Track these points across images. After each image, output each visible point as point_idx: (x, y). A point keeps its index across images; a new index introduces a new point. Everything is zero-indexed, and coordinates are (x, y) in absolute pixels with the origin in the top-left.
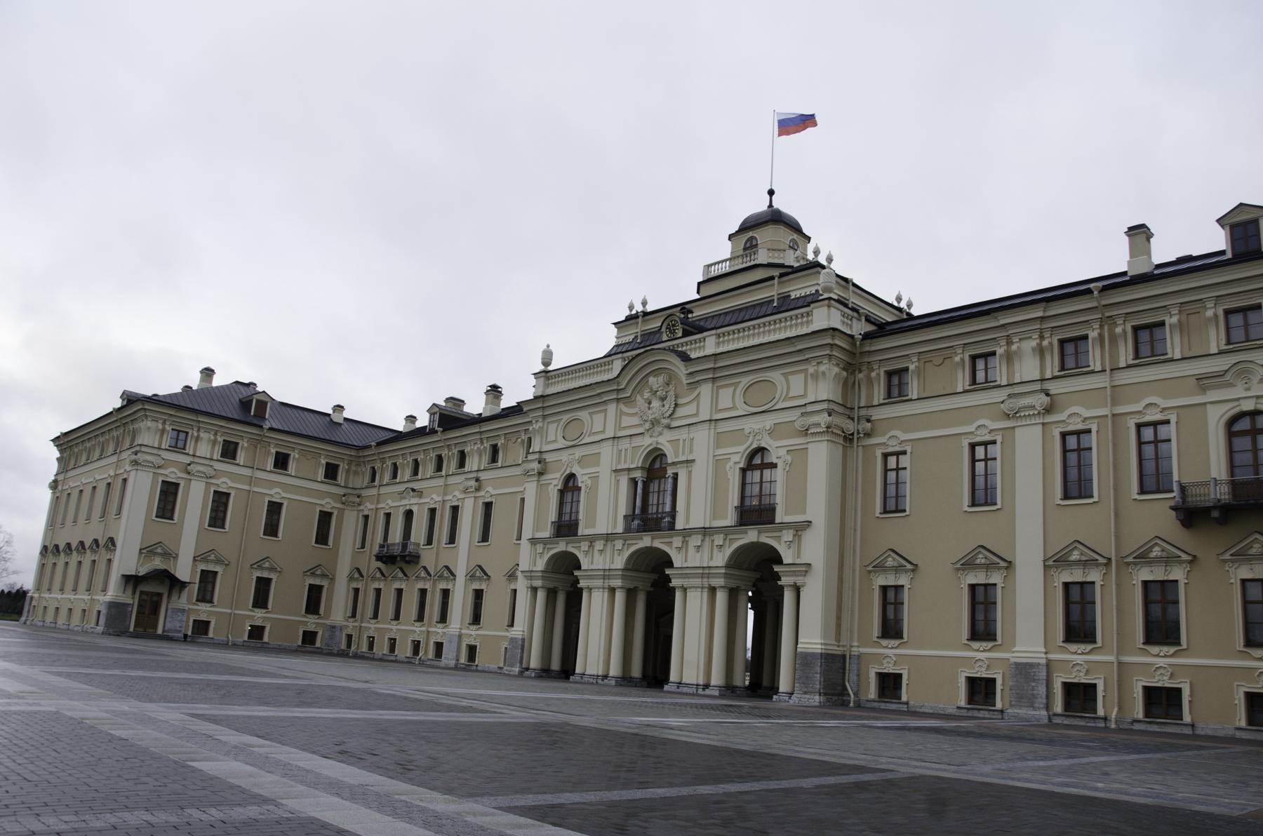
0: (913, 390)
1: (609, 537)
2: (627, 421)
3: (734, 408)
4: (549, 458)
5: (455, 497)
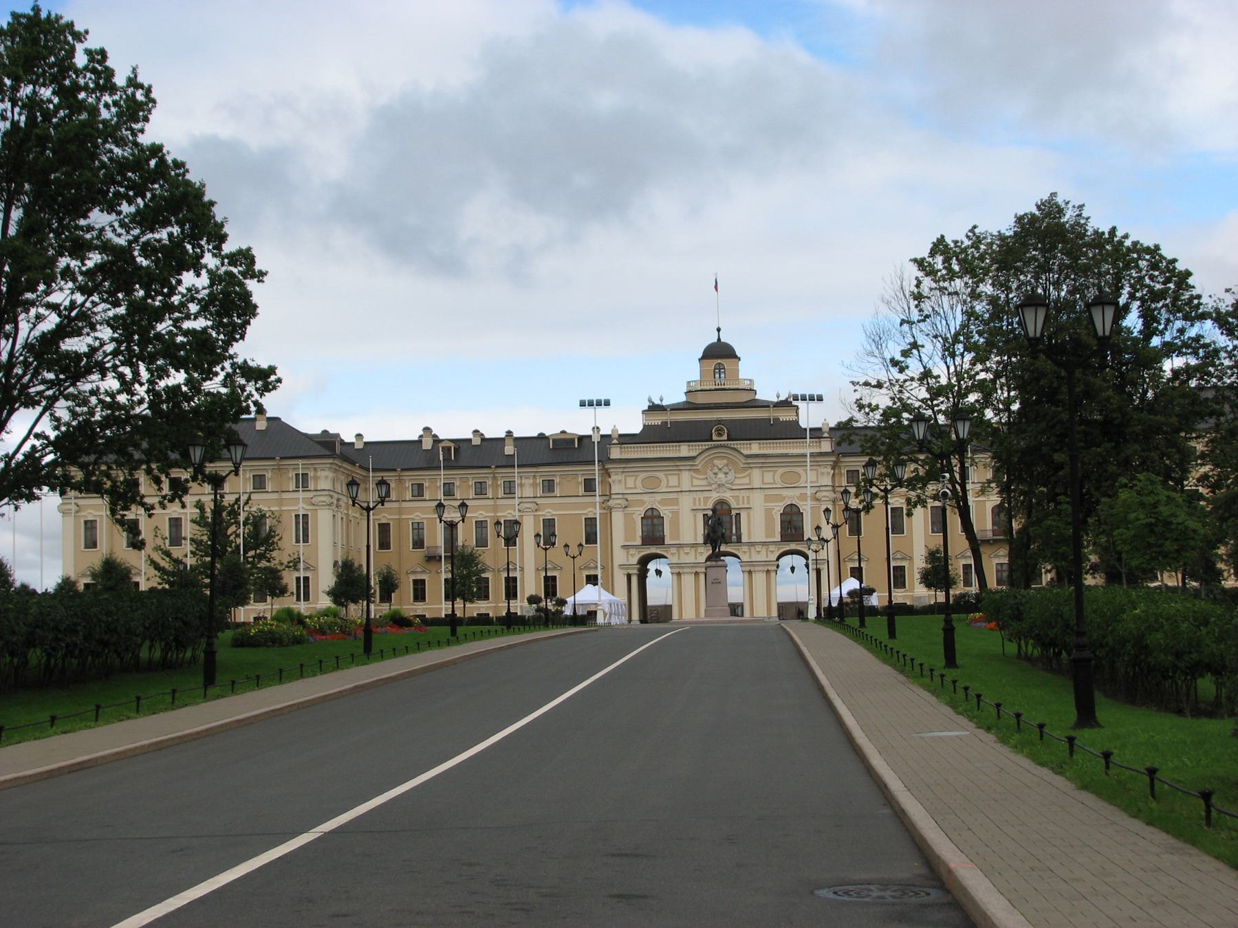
1: (694, 545)
2: (696, 482)
3: (774, 483)
4: (630, 498)
5: (508, 514)
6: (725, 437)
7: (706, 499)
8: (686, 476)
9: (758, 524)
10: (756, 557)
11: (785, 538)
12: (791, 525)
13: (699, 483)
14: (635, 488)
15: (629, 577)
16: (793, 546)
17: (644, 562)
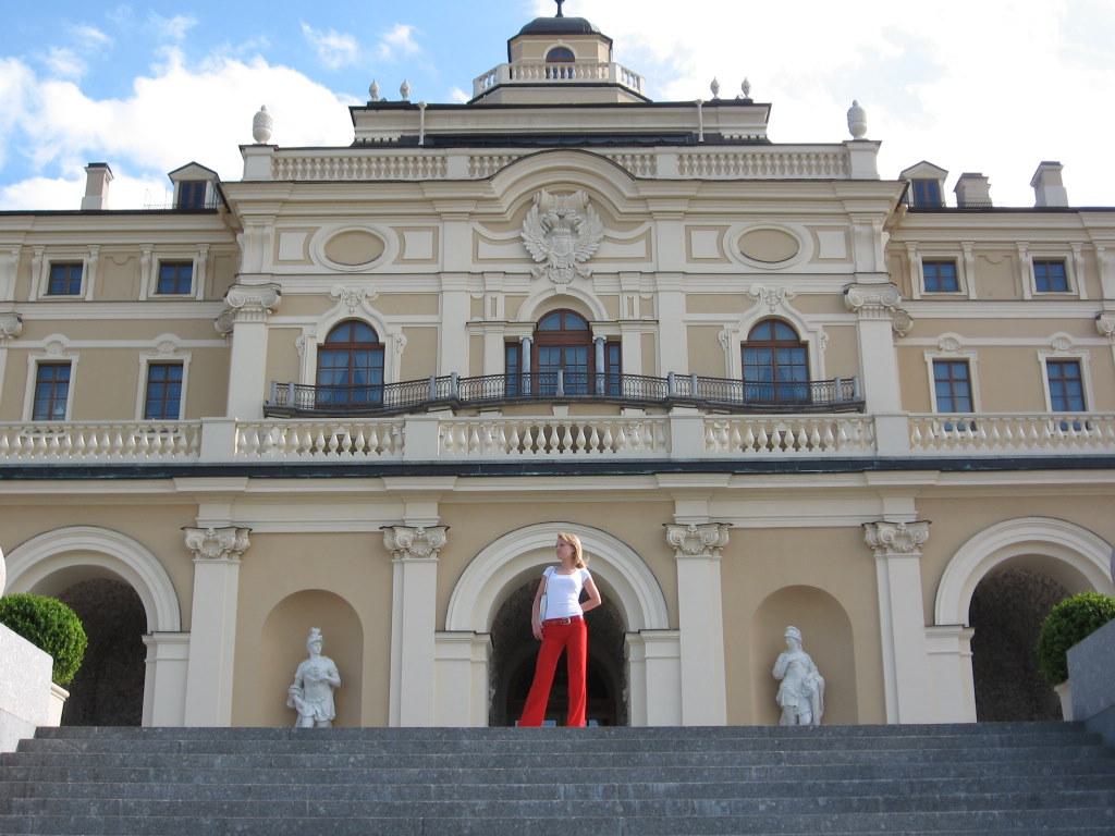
2: (486, 250)
4: (289, 287)
7: (516, 299)
13: (499, 249)
14: (308, 260)
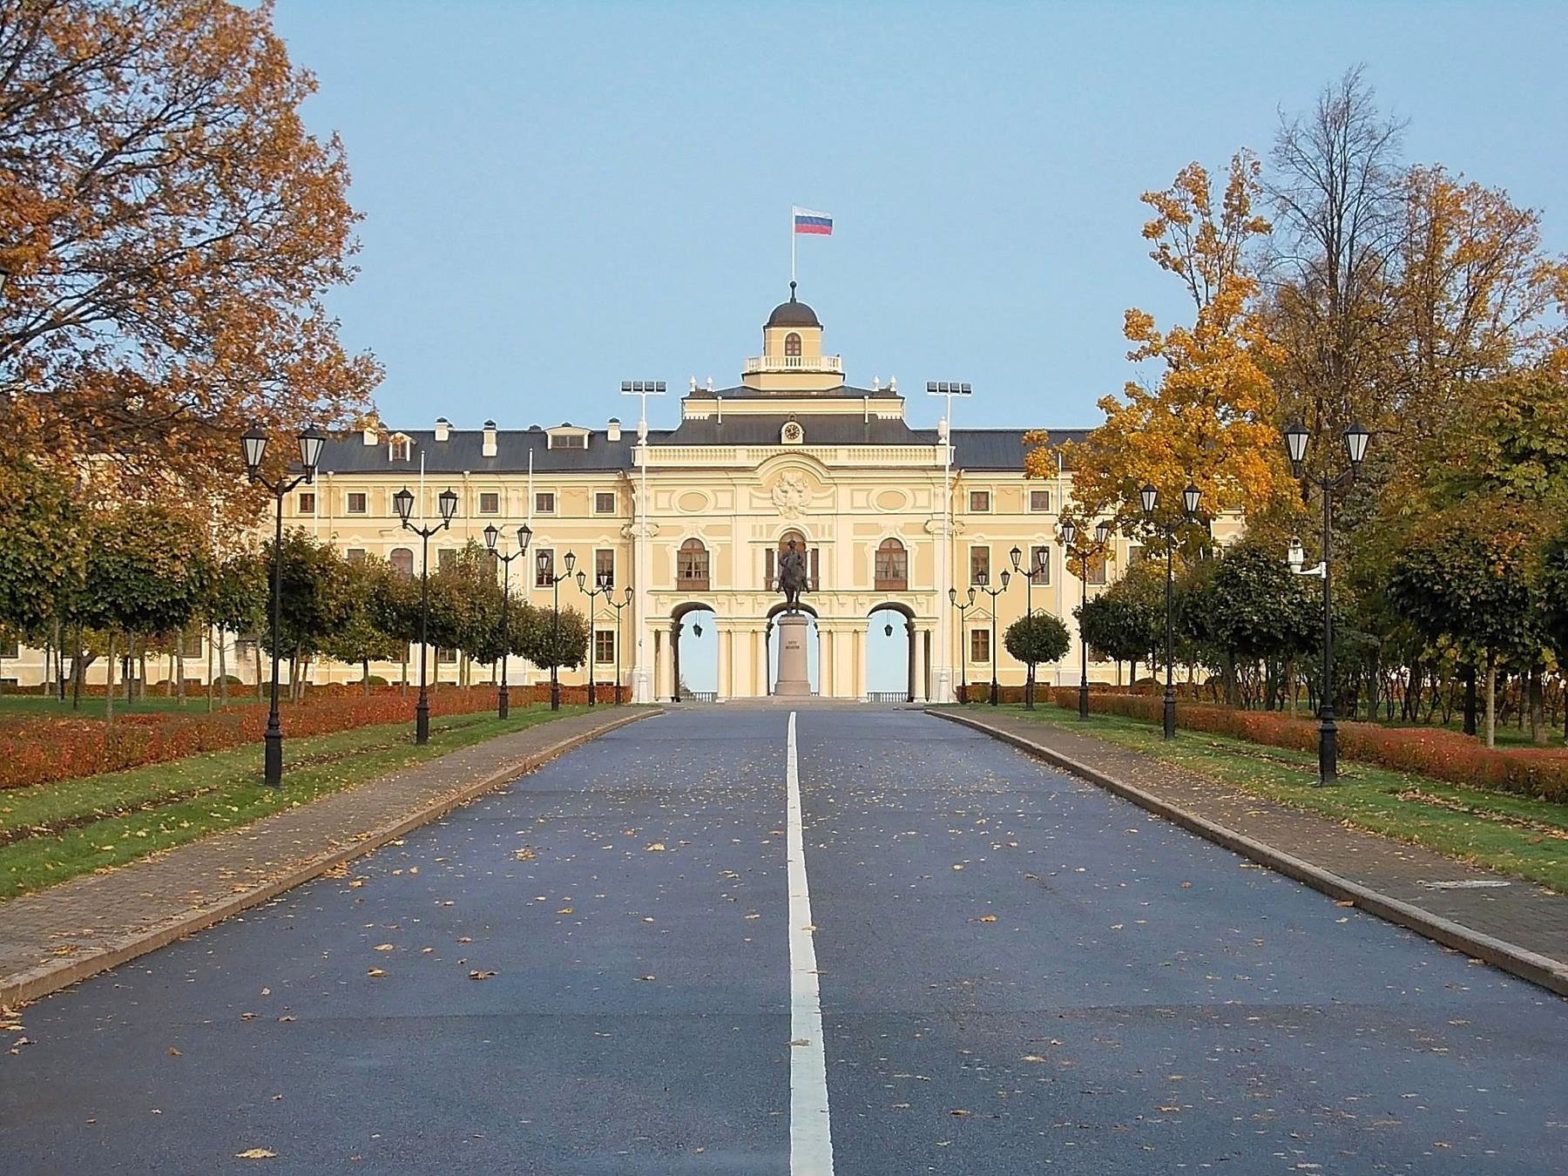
0: (993, 506)
2: (756, 503)
6: (800, 439)
7: (771, 527)
8: (743, 494)
9: (843, 568)
10: (838, 612)
11: (881, 586)
12: (891, 567)
15: (658, 634)
16: (893, 598)
17: (679, 613)
